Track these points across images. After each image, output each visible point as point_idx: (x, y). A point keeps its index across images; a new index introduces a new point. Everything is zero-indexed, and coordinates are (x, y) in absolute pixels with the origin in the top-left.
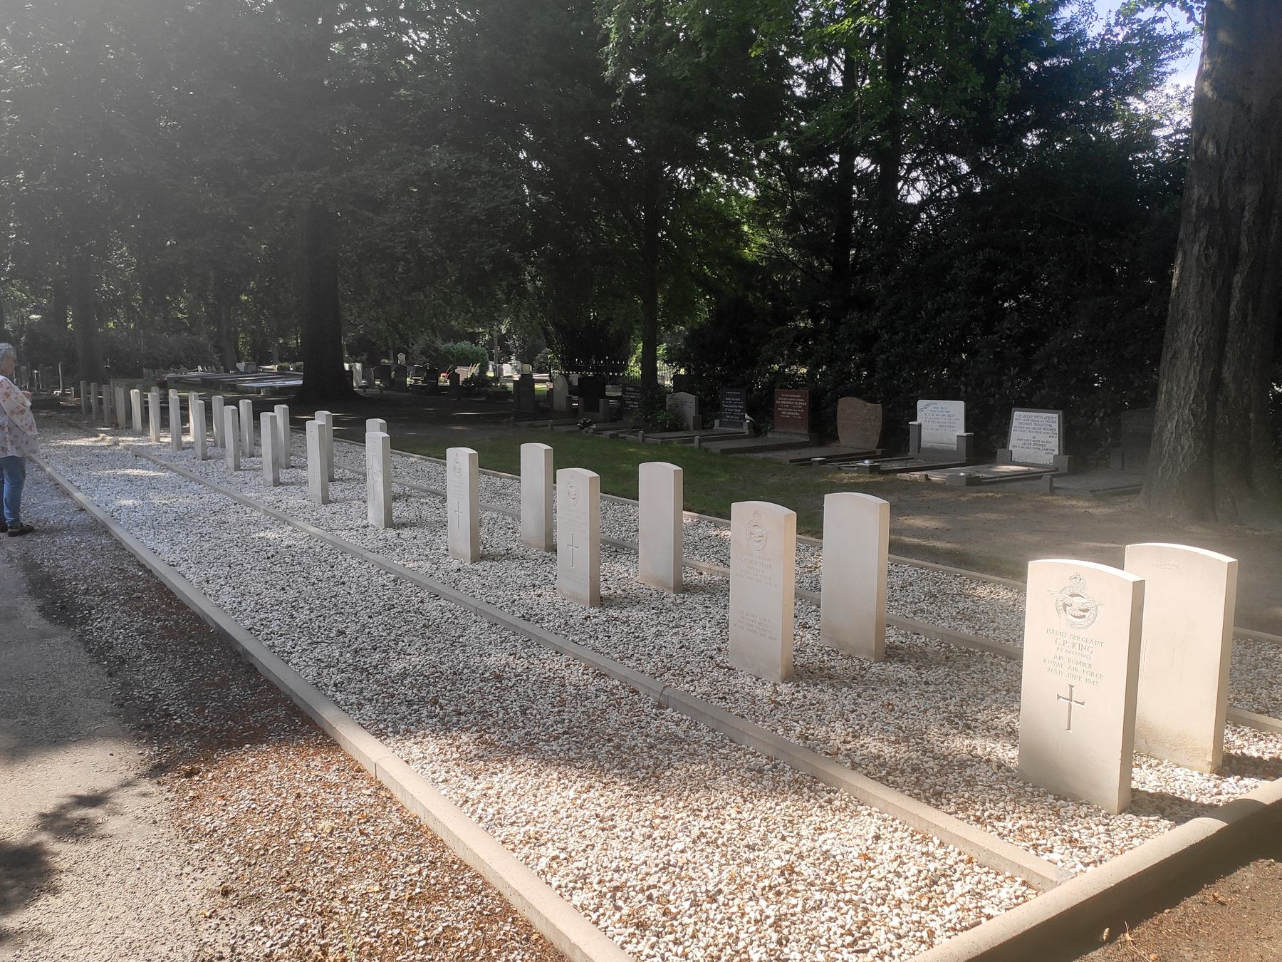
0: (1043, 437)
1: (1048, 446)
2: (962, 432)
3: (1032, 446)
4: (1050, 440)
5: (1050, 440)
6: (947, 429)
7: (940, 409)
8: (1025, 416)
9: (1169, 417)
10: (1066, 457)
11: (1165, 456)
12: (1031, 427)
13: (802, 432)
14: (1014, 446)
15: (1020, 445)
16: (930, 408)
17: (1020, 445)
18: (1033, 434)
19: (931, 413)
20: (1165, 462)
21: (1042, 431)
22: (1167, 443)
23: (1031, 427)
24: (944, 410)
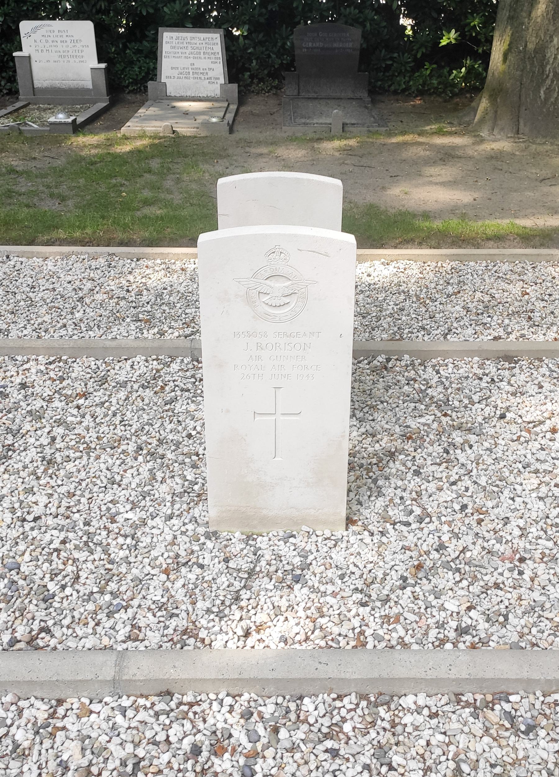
0: (203, 64)
1: (211, 74)
4: (212, 66)
5: (212, 66)
6: (72, 60)
7: (56, 33)
8: (178, 38)
9: (555, 30)
10: (235, 86)
11: (548, 76)
15: (176, 76)
16: (43, 31)
17: (176, 76)
18: (191, 61)
19: (44, 39)
20: (548, 82)
21: (202, 55)
22: (551, 61)
24: (64, 35)
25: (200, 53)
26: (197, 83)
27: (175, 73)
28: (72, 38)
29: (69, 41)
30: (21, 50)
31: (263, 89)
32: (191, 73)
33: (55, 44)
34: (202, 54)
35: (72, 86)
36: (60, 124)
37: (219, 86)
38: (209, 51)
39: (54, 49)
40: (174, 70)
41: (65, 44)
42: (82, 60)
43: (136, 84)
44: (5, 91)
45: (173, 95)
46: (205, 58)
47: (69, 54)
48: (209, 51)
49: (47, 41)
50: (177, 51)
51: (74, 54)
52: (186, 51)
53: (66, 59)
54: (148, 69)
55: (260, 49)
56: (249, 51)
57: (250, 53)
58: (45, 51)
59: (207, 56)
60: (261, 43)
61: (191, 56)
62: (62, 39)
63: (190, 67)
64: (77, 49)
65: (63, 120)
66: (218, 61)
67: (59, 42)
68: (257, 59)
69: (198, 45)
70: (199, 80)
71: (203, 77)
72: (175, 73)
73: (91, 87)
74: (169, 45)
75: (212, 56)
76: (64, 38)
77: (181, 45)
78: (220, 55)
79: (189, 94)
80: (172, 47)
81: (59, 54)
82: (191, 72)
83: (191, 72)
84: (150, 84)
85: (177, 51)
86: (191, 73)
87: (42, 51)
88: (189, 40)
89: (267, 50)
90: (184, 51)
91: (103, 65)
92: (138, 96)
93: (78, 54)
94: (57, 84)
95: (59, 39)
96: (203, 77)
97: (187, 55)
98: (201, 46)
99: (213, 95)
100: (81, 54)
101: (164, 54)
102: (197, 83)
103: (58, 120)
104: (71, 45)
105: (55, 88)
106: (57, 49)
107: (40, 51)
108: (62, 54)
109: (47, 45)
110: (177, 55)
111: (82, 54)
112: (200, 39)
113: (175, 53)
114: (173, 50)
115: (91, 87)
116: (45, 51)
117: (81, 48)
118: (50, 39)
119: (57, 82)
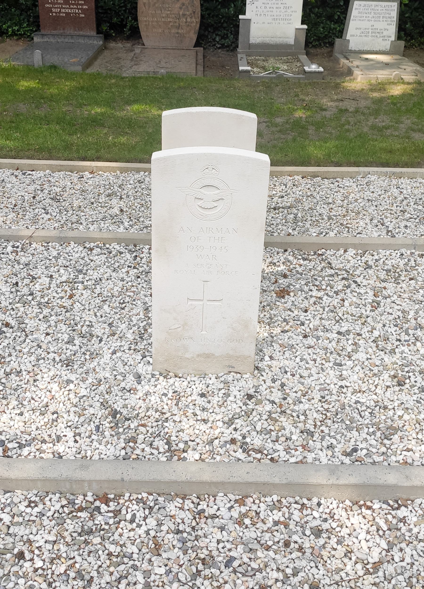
0: (381, 25)
1: (385, 33)
2: (299, 25)
3: (370, 34)
4: (387, 27)
5: (387, 27)
6: (282, 22)
12: (370, 16)
13: (88, 34)
14: (351, 36)
15: (358, 34)
17: (358, 34)
18: (372, 23)
19: (264, 5)
21: (381, 19)
23: (370, 16)
25: (380, 17)
26: (374, 40)
27: (358, 32)
28: (285, 6)
29: (282, 8)
30: (244, 14)
31: (413, 45)
32: (370, 33)
33: (271, 9)
34: (381, 17)
35: (278, 42)
36: (315, 72)
37: (389, 42)
38: (388, 15)
39: (270, 13)
40: (358, 30)
41: (278, 10)
42: (289, 22)
43: (318, 40)
44: (219, 46)
45: (353, 49)
46: (383, 21)
47: (281, 18)
48: (388, 15)
49: (265, 7)
50: (363, 15)
51: (285, 18)
52: (369, 15)
53: (277, 22)
54: (330, 29)
55: (416, 14)
56: (407, 15)
57: (407, 17)
58: (262, 15)
59: (385, 19)
60: (416, 9)
61: (373, 19)
62: (277, 6)
63: (370, 28)
64: (287, 13)
65: (317, 70)
66: (393, 23)
67: (275, 8)
68: (411, 22)
69: (379, 11)
70: (375, 38)
71: (379, 35)
72: (358, 32)
73: (293, 43)
74: (357, 11)
75: (389, 20)
76: (280, 5)
77: (366, 11)
78: (395, 19)
79: (366, 48)
80: (359, 13)
81: (273, 17)
82: (370, 31)
83: (370, 31)
84: (338, 41)
85: (363, 15)
86: (370, 33)
87: (261, 15)
88: (373, 7)
89: (419, 15)
90: (368, 15)
91: (305, 27)
92: (318, 50)
93: (287, 18)
94: (267, 40)
95: (275, 6)
96: (379, 35)
97: (370, 18)
98: (382, 11)
99: (384, 49)
100: (289, 18)
101: (352, 17)
102: (374, 40)
103: (314, 70)
104: (283, 10)
105: (265, 43)
107: (259, 15)
108: (275, 17)
109: (266, 10)
110: (362, 19)
111: (291, 17)
112: (381, 6)
113: (361, 17)
114: (360, 15)
115: (293, 43)
116: (262, 15)
117: (291, 13)
118: (268, 6)
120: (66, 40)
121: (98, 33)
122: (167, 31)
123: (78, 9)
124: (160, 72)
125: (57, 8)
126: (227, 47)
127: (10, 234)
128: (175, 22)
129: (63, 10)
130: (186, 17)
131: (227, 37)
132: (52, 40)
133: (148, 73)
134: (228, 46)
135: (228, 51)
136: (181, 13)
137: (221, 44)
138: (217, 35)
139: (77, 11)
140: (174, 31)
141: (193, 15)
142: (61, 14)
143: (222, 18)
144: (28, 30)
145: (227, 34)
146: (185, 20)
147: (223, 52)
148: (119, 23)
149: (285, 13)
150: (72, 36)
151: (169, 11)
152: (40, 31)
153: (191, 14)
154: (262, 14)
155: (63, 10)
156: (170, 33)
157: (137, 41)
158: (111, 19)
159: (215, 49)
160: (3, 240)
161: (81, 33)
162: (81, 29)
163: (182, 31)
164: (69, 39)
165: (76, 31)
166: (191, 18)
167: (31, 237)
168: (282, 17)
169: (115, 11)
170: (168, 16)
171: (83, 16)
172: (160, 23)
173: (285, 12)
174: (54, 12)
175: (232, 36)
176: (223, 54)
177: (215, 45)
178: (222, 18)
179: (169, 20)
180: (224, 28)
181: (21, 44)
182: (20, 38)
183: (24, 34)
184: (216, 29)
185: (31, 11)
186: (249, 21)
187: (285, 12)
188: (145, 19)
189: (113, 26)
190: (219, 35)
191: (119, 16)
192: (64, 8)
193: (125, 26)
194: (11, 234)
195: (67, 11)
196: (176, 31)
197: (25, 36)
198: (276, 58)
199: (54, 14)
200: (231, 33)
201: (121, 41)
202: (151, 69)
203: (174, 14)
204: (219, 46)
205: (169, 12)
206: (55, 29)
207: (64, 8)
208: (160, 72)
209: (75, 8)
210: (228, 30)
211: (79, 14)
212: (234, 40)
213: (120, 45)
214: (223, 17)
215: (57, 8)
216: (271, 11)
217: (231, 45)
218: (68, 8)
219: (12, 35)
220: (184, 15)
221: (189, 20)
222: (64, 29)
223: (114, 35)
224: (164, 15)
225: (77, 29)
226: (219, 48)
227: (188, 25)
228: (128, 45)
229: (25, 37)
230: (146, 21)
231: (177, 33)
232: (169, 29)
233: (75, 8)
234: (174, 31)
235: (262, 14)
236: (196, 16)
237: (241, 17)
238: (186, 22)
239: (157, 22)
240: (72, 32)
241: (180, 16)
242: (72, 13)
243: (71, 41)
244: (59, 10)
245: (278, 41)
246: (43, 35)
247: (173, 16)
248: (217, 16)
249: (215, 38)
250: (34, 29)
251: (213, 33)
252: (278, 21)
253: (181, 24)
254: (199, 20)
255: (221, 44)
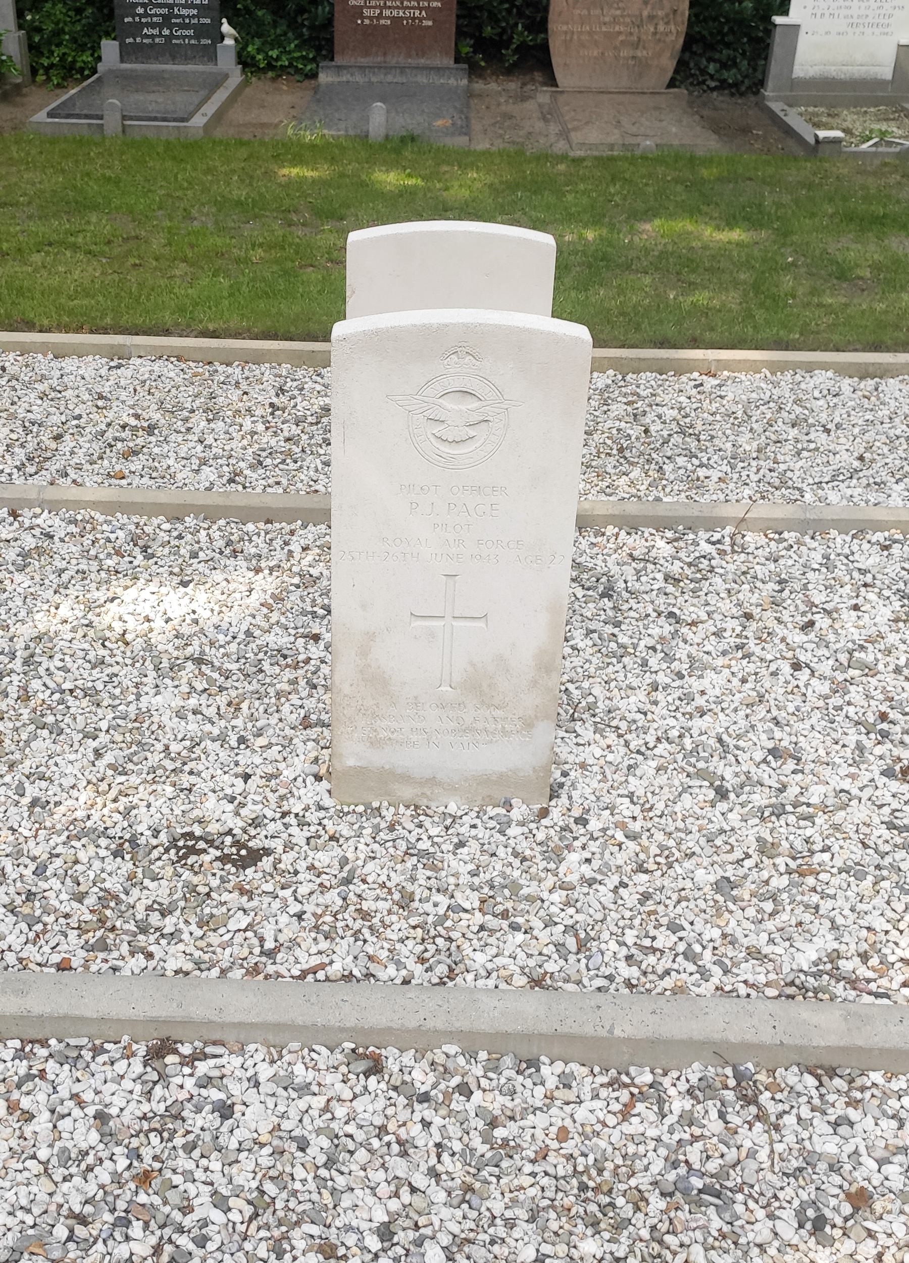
6: (868, 31)
30: (786, 13)
35: (856, 76)
39: (844, 12)
42: (886, 30)
44: (713, 84)
47: (867, 21)
51: (876, 21)
58: (827, 15)
64: (883, 12)
73: (889, 77)
81: (851, 21)
87: (823, 15)
93: (882, 21)
94: (833, 71)
100: (886, 21)
105: (827, 78)
106: (849, 12)
107: (818, 16)
108: (855, 20)
115: (889, 77)
116: (827, 15)
119: (833, 68)
120: (390, 78)
121: (457, 61)
122: (610, 54)
123: (421, 9)
124: (643, 144)
125: (375, 7)
126: (730, 86)
127: (696, 514)
128: (631, 34)
129: (387, 13)
130: (655, 21)
131: (735, 64)
132: (359, 78)
133: (612, 147)
134: (736, 85)
135: (732, 95)
136: (645, 13)
137: (719, 81)
138: (710, 60)
139: (417, 14)
140: (625, 53)
141: (671, 16)
142: (382, 22)
143: (725, 23)
144: (298, 58)
145: (734, 60)
146: (652, 29)
147: (721, 98)
148: (496, 38)
149: (878, 12)
150: (402, 70)
151: (619, 8)
152: (332, 59)
153: (667, 15)
154: (827, 13)
155: (387, 13)
156: (616, 58)
157: (528, 77)
158: (480, 27)
159: (704, 91)
160: (681, 527)
161: (422, 61)
162: (422, 53)
163: (645, 52)
164: (395, 76)
165: (410, 56)
166: (667, 23)
167: (743, 520)
168: (870, 20)
169: (490, 12)
170: (615, 21)
171: (430, 23)
172: (596, 37)
173: (879, 8)
174: (367, 17)
175: (745, 62)
176: (723, 102)
177: (704, 82)
178: (725, 23)
179: (617, 28)
180: (728, 45)
181: (285, 88)
182: (280, 76)
183: (291, 65)
184: (712, 47)
185: (306, 16)
186: (796, 27)
187: (879, 8)
188: (565, 28)
189: (481, 45)
190: (714, 61)
191: (497, 21)
192: (390, 7)
193: (507, 44)
194: (699, 514)
195: (395, 13)
196: (631, 53)
197: (289, 70)
198: (852, 109)
199: (367, 22)
200: (744, 54)
201: (494, 78)
202: (615, 137)
203: (629, 15)
204: (713, 84)
205: (618, 12)
206: (367, 54)
207: (390, 7)
208: (643, 144)
209: (412, 8)
210: (735, 50)
211: (421, 20)
212: (750, 71)
213: (493, 86)
214: (728, 21)
215: (375, 7)
216: (846, 7)
217: (743, 82)
218: (398, 8)
219: (264, 71)
220: (651, 18)
221: (661, 28)
222: (385, 54)
223: (483, 64)
224: (607, 19)
225: (414, 53)
226: (713, 89)
227: (659, 40)
228: (513, 85)
229: (289, 73)
230: (566, 33)
231: (634, 58)
232: (615, 48)
233: (412, 8)
234: (625, 53)
235: (827, 13)
236: (679, 19)
237: (778, 20)
238: (655, 34)
239: (590, 33)
240: (401, 60)
241: (642, 21)
242: (407, 19)
243: (399, 79)
244: (378, 11)
245: (856, 71)
246: (339, 68)
247: (628, 20)
248: (715, 19)
249: (706, 67)
250: (311, 56)
251: (701, 55)
252: (861, 28)
253: (644, 37)
254: (683, 28)
255: (719, 81)
